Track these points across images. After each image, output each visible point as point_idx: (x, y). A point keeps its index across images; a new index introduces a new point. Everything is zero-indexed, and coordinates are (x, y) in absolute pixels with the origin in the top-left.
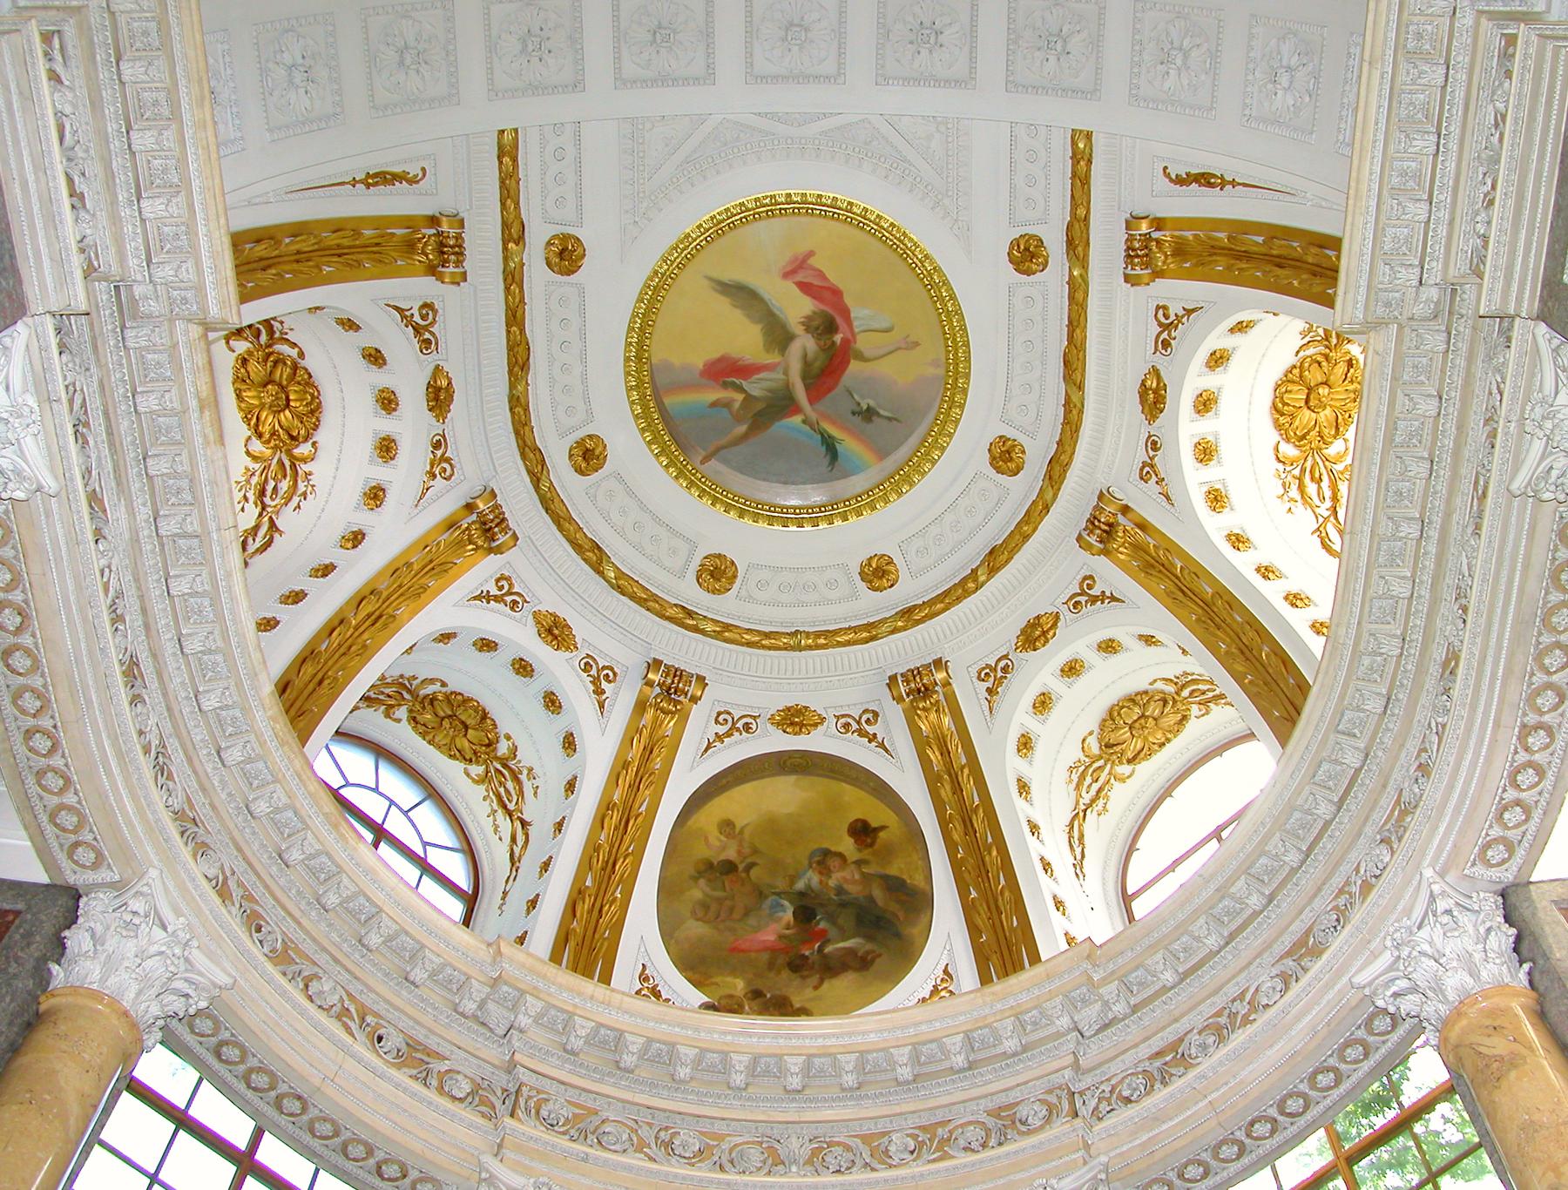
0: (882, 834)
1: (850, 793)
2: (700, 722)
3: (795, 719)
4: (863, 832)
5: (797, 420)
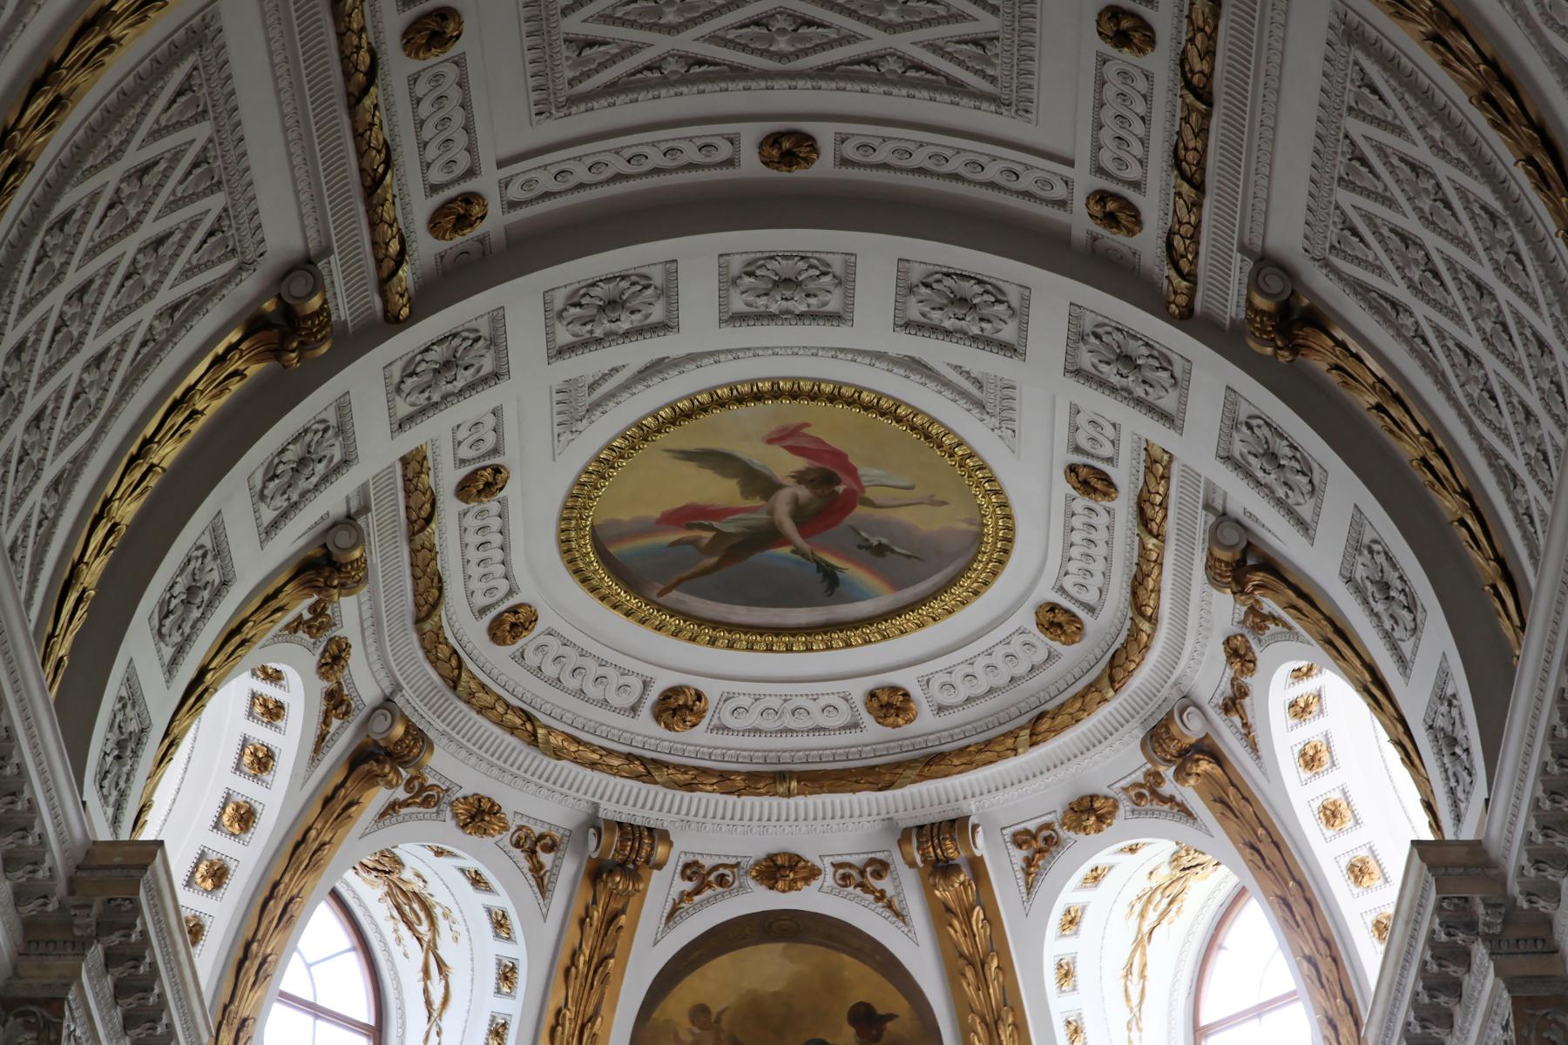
0: (890, 1026)
1: (852, 968)
2: (662, 887)
3: (780, 869)
4: (866, 1019)
5: (785, 551)
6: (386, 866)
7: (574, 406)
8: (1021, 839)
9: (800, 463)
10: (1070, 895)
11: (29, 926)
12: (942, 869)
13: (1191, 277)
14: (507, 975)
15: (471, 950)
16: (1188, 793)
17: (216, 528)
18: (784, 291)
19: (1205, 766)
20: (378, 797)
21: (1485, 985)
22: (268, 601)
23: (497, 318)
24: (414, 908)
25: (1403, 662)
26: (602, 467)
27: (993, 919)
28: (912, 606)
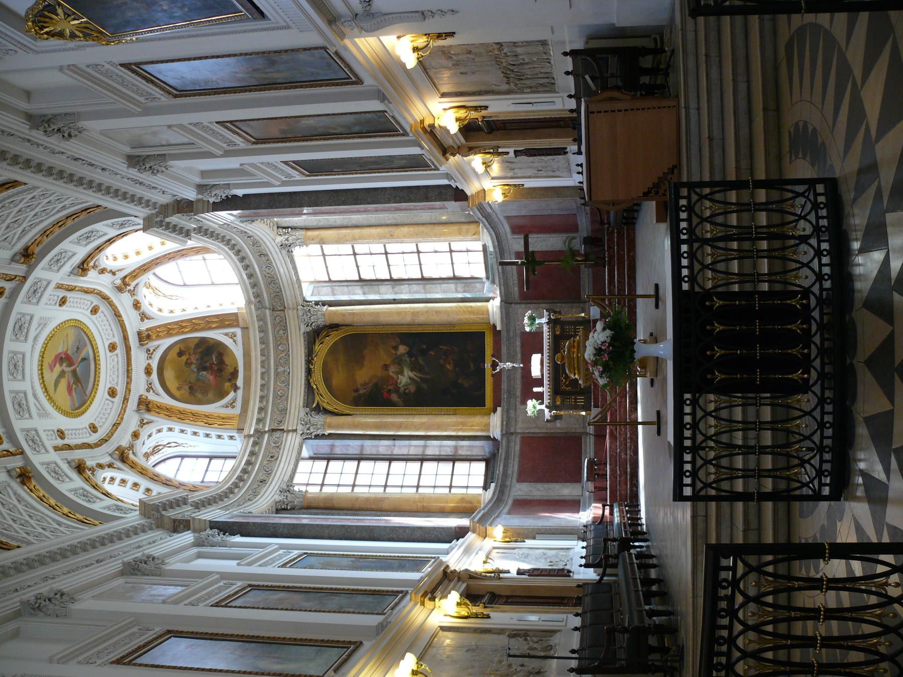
1: (169, 357)
2: (151, 397)
3: (148, 372)
4: (180, 354)
6: (147, 456)
7: (44, 414)
8: (142, 320)
9: (58, 365)
11: (158, 527)
12: (149, 337)
13: (16, 276)
14: (170, 429)
15: (164, 437)
16: (133, 284)
17: (70, 491)
18: (17, 368)
19: (127, 279)
20: (131, 456)
21: (174, 219)
22: (87, 480)
23: (22, 430)
24: (156, 450)
25: (105, 234)
26: (58, 408)
27: (159, 326)
28: (91, 342)
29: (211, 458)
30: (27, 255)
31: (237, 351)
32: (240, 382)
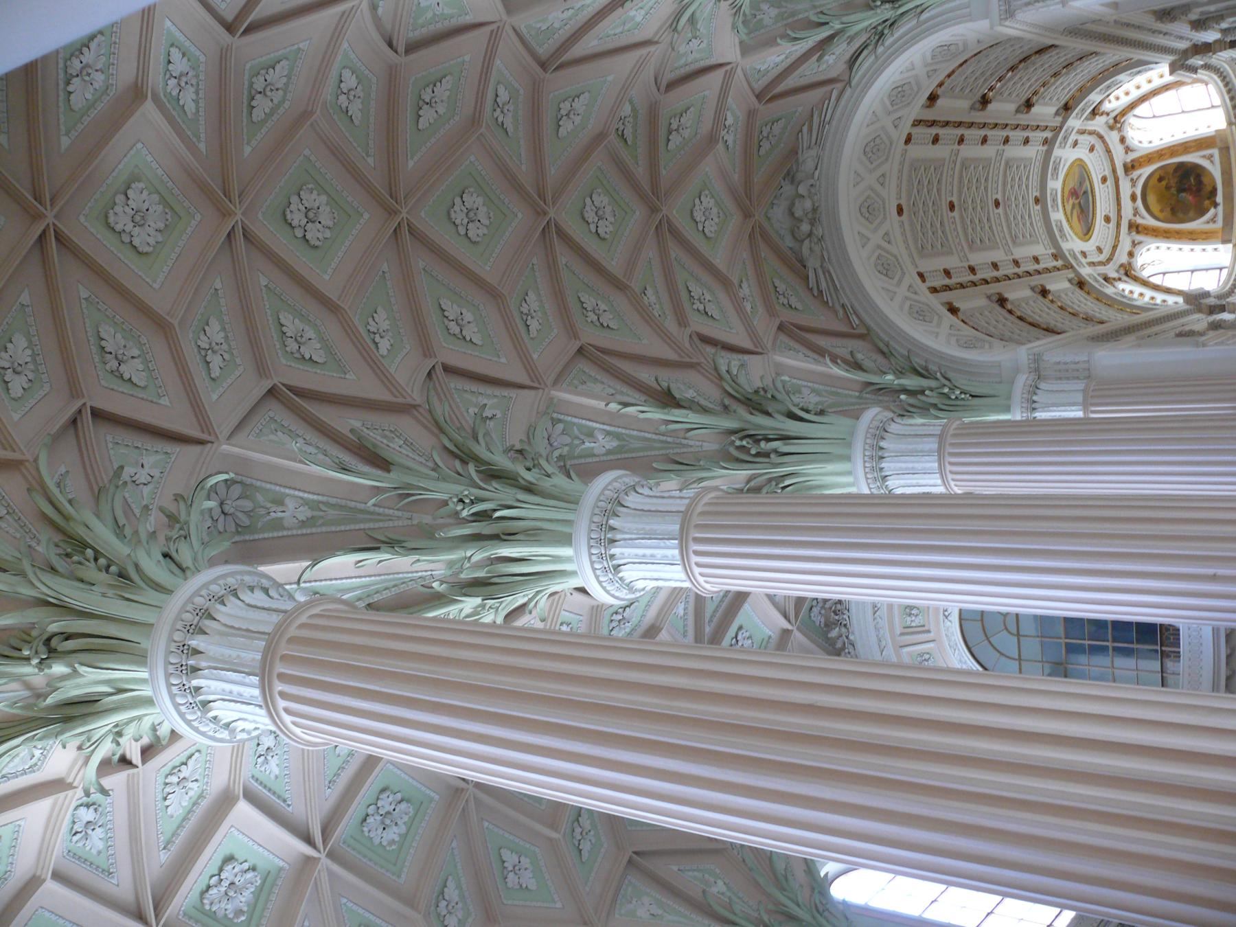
1: (1151, 183)
2: (1139, 221)
3: (1133, 198)
4: (1160, 180)
10: (1136, 143)
12: (1133, 167)
29: (1192, 271)
30: (1067, 108)
31: (1216, 171)
32: (1219, 199)
